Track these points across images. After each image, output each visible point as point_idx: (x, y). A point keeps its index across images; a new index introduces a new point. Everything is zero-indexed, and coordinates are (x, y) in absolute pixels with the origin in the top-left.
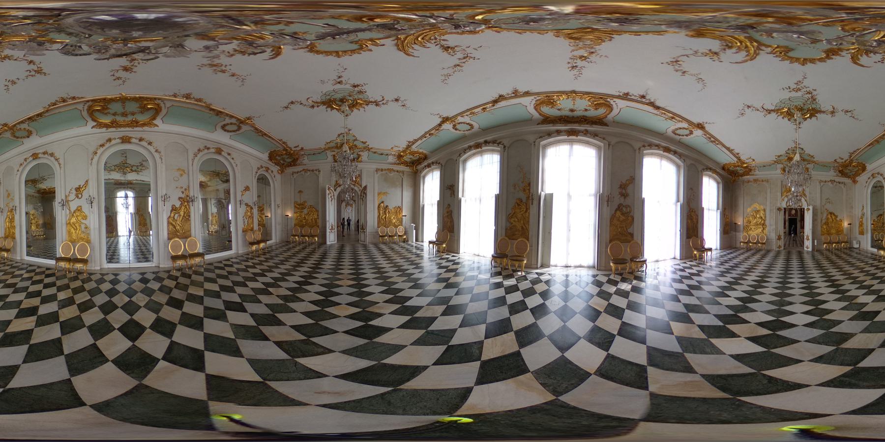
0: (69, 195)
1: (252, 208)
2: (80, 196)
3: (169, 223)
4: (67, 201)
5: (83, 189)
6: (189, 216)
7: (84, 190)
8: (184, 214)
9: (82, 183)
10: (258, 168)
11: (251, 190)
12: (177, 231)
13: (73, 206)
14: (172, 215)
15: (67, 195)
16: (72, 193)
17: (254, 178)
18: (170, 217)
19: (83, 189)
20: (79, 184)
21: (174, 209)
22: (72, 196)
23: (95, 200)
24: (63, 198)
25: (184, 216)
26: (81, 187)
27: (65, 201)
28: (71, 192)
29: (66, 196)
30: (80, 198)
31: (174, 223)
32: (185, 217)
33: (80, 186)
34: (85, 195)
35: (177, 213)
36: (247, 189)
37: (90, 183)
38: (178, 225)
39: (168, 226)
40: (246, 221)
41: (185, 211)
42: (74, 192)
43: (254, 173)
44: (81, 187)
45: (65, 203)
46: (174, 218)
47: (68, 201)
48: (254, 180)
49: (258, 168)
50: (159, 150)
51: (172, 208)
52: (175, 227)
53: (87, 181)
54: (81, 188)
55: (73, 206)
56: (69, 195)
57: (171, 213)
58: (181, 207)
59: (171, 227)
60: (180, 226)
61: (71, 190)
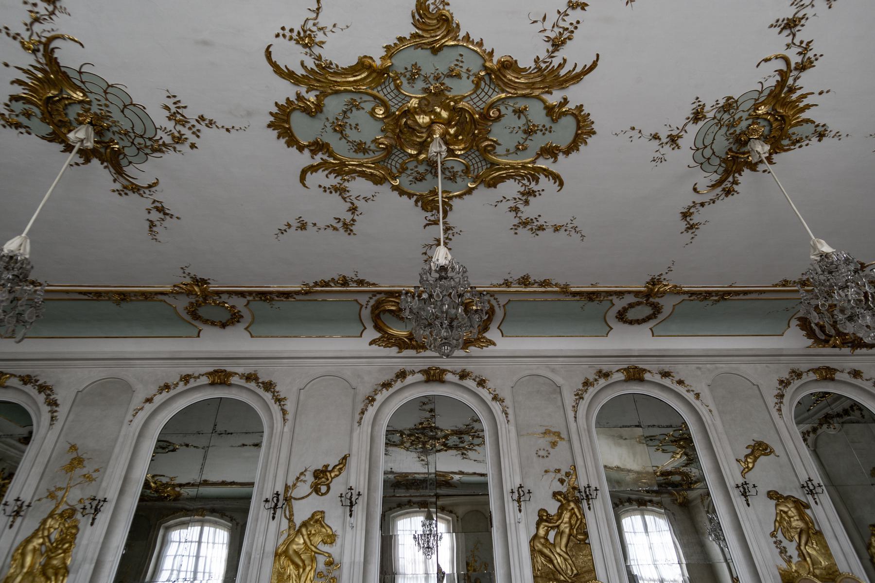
0: (294, 485)
1: (801, 506)
2: (324, 489)
3: (533, 550)
4: (287, 500)
5: (333, 475)
6: (586, 534)
7: (337, 476)
8: (571, 528)
9: (333, 461)
10: (781, 382)
11: (778, 449)
12: (557, 571)
13: (302, 511)
14: (542, 532)
15: (290, 483)
16: (305, 481)
17: (775, 414)
18: (536, 537)
19: (333, 475)
20: (326, 464)
21: (543, 517)
22: (304, 489)
23: (360, 498)
24: (280, 488)
25: (570, 535)
26: (330, 468)
27: (281, 498)
28: (302, 477)
29: (287, 488)
30: (323, 494)
31: (546, 551)
32: (575, 537)
33: (326, 466)
34: (338, 486)
35: (552, 528)
36: (759, 449)
37: (353, 462)
38: (560, 555)
39: (533, 558)
40: (792, 550)
41: (573, 522)
42: (310, 478)
43: (771, 401)
44: (330, 468)
45: (280, 505)
46: (547, 540)
47: (291, 497)
48: (780, 423)
49: (781, 382)
50: (501, 396)
51: (540, 516)
52: (551, 561)
53: (345, 458)
54: (330, 472)
55: (302, 511)
56: (294, 485)
57: (538, 528)
58: (562, 513)
59: (541, 559)
60: (565, 560)
61: (302, 474)
